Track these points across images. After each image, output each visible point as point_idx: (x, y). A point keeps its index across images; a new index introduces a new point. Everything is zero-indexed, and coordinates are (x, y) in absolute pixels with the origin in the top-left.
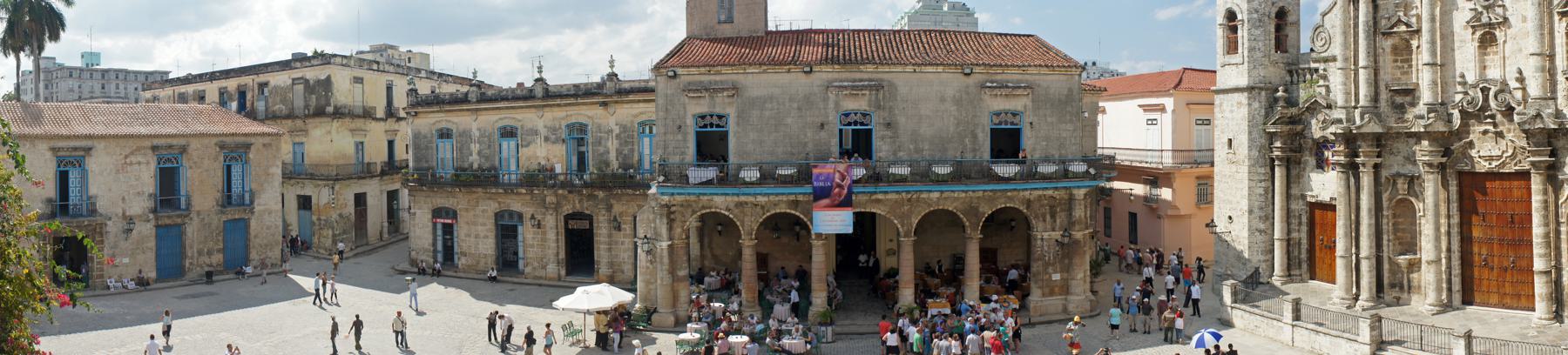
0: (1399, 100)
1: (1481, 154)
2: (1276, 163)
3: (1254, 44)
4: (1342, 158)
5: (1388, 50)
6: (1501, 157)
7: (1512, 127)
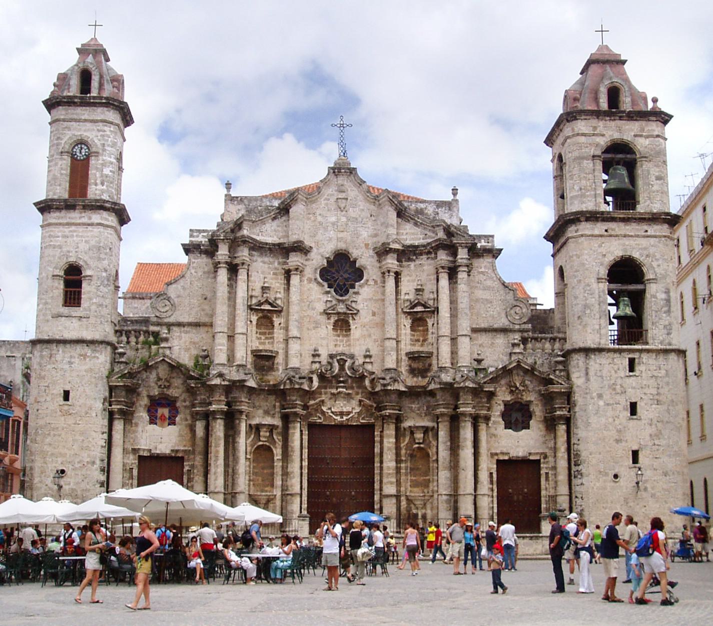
1: (333, 410)
3: (101, 301)
4: (223, 407)
5: (254, 323)
6: (352, 412)
7: (360, 391)
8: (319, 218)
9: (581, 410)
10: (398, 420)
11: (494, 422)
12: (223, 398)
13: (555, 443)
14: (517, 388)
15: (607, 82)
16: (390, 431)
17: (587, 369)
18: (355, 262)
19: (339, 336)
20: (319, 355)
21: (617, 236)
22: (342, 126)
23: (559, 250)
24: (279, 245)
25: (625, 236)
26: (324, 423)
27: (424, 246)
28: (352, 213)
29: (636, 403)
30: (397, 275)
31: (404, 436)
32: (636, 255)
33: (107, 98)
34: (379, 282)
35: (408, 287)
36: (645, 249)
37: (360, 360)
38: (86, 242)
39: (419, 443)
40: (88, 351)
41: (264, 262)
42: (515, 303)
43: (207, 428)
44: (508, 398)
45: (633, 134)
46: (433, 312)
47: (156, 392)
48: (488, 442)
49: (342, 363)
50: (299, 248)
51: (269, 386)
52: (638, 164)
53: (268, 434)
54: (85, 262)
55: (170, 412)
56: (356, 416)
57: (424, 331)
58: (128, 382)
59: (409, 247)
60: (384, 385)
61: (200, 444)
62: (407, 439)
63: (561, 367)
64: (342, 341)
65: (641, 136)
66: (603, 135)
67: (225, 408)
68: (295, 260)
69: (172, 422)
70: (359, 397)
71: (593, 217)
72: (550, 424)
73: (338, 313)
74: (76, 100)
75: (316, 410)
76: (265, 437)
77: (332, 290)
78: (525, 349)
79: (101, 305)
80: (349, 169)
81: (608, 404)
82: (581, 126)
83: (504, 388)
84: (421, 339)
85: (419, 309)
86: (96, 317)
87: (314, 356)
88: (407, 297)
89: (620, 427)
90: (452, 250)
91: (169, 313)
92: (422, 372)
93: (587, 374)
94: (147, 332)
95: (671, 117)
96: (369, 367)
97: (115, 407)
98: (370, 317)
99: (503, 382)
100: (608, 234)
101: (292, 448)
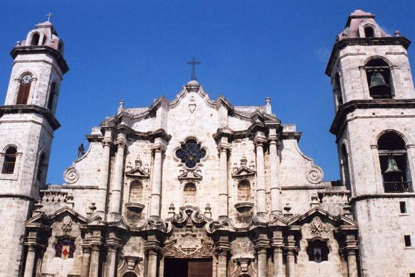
0: (132, 213)
1: (183, 247)
2: (30, 249)
3: (27, 170)
5: (129, 185)
6: (195, 249)
7: (202, 233)
8: (177, 118)
9: (367, 242)
10: (229, 255)
11: (301, 256)
12: (99, 235)
13: (348, 270)
14: (317, 229)
15: (364, 24)
16: (223, 260)
17: (369, 211)
18: (199, 145)
19: (188, 195)
20: (174, 209)
21: (381, 117)
22: (194, 63)
23: (340, 136)
24: (148, 133)
25: (387, 117)
26: (176, 257)
27: (246, 131)
28: (197, 113)
29: (409, 236)
30: (229, 152)
31: (233, 266)
32: (397, 129)
33: (45, 47)
34: (217, 156)
35: (235, 159)
36: (404, 125)
37: (202, 211)
38: (22, 132)
39: (245, 271)
40: (14, 202)
41: (138, 146)
42: (312, 169)
43: (90, 258)
44: (311, 237)
45: (384, 53)
46: (253, 175)
47: (62, 234)
48: (295, 269)
49: (189, 212)
50: (162, 135)
51: (136, 229)
52: (391, 71)
53: (134, 264)
54: (19, 144)
55: (70, 249)
56: (199, 251)
57: (247, 190)
58: (38, 225)
59: (235, 132)
60: (217, 227)
61: (85, 270)
62: (236, 268)
63: (348, 212)
64: (190, 199)
65: (391, 53)
66: (365, 54)
67: (98, 241)
68: (158, 141)
69: (71, 256)
70: (202, 237)
71: (363, 105)
72: (344, 255)
73: (188, 179)
74: (27, 49)
75: (170, 247)
76: (132, 266)
77: (184, 164)
78: (321, 202)
79: (27, 172)
80: (196, 86)
81: (387, 237)
82: (349, 49)
83: (307, 230)
84: (246, 195)
85: (244, 173)
86: (22, 180)
87: (170, 209)
88: (235, 166)
89: (398, 255)
90: (265, 130)
91: (75, 180)
92: (246, 219)
93: (369, 215)
94: (59, 193)
95: (410, 42)
96: (208, 216)
97: (30, 243)
98: (210, 181)
99: (306, 225)
100: (374, 116)
101: (150, 274)
